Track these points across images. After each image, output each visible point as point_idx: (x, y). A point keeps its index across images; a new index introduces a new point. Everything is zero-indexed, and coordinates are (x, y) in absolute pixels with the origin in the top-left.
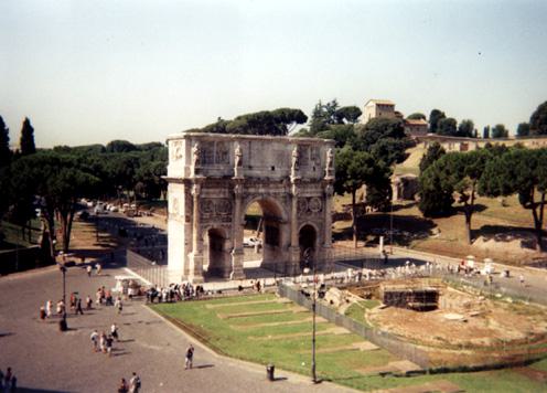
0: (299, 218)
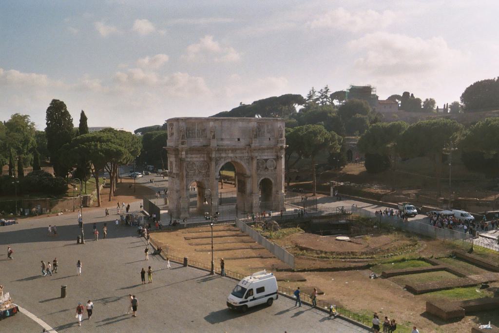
0: (258, 175)
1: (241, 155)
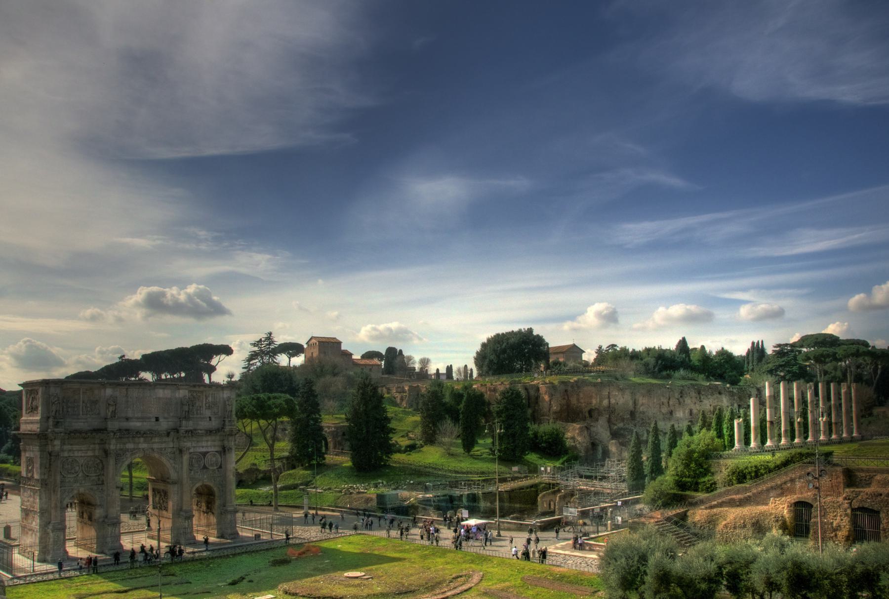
1: (163, 446)
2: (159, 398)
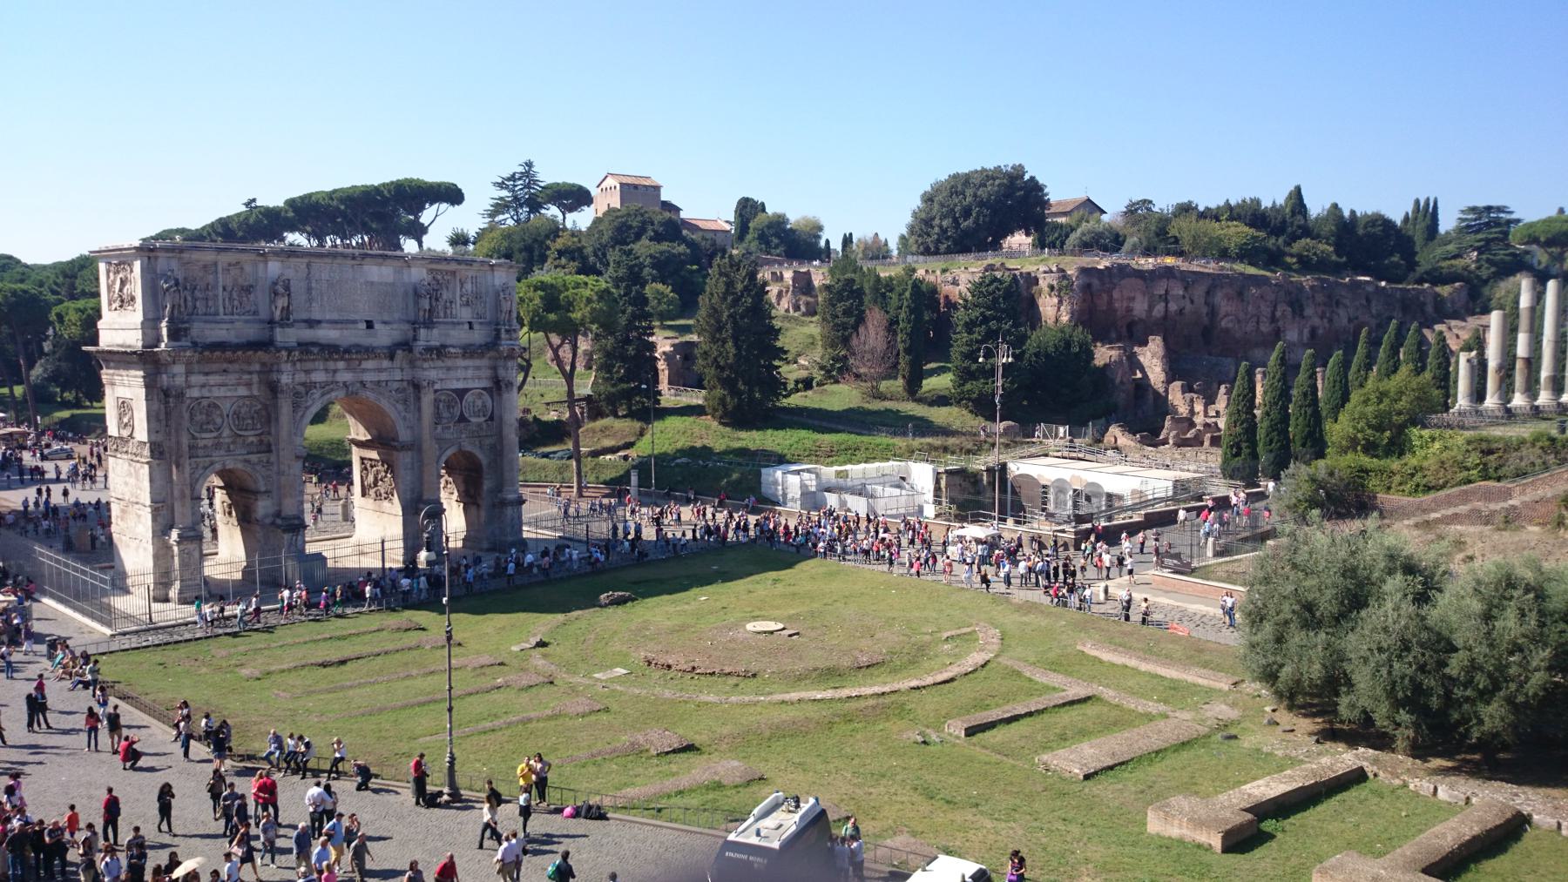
0: (439, 440)
1: (384, 376)
2: (372, 283)
